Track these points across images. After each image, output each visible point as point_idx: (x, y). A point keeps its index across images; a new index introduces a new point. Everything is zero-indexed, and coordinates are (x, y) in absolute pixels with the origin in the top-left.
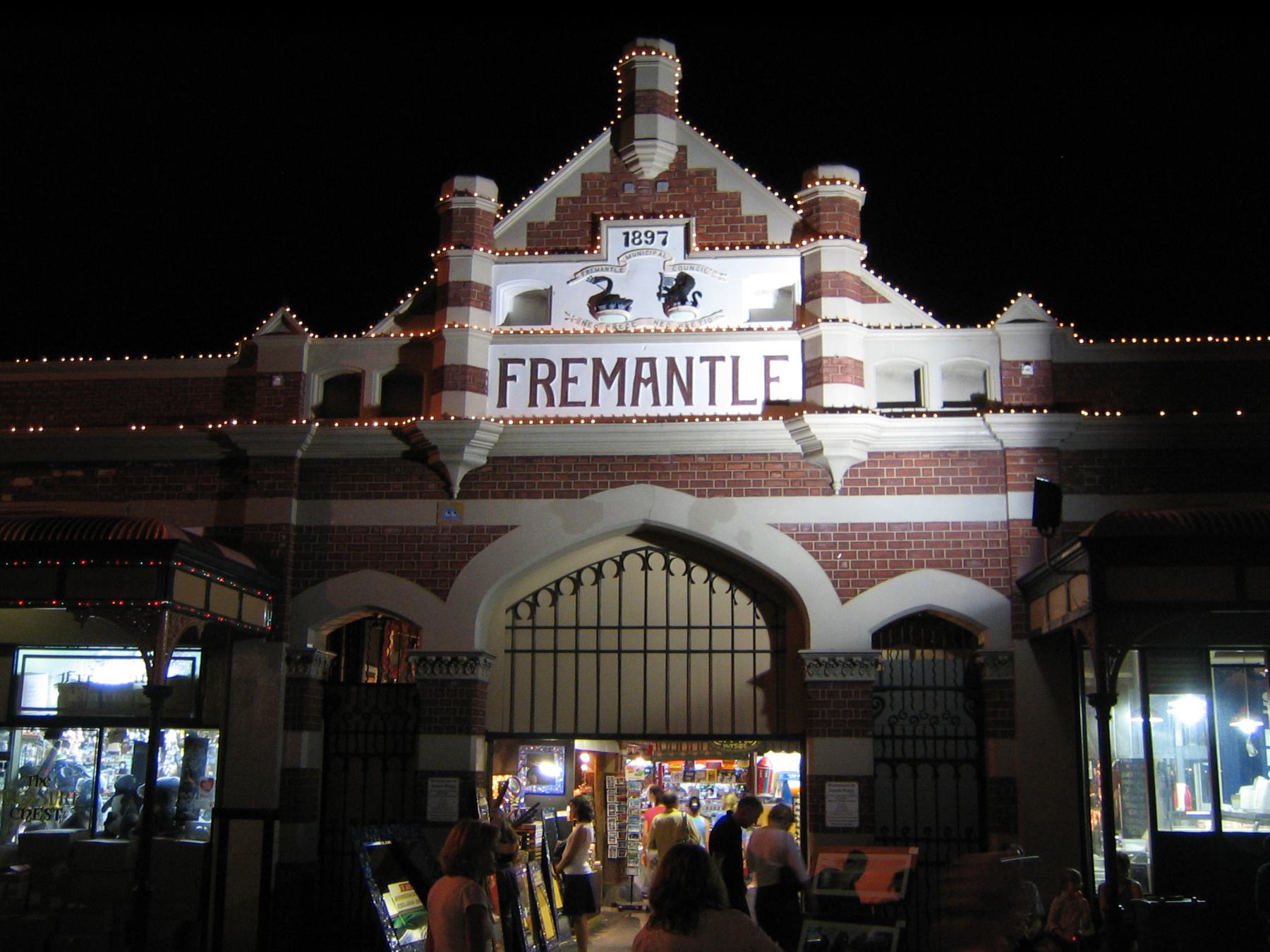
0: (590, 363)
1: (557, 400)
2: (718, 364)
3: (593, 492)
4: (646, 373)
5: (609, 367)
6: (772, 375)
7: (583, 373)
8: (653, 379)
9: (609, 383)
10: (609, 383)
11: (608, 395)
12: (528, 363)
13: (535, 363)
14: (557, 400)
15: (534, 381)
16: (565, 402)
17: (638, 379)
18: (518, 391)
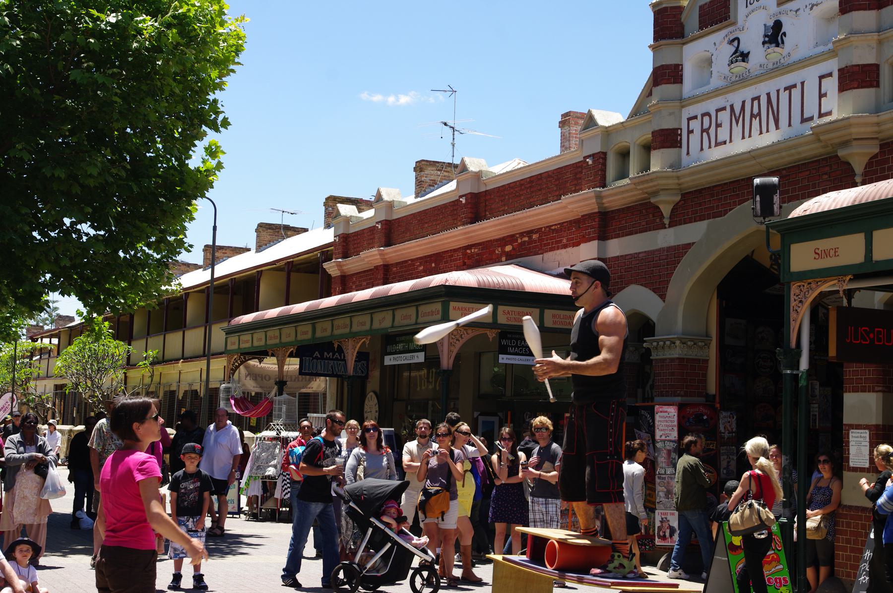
0: (728, 109)
1: (713, 143)
2: (793, 91)
3: (730, 210)
4: (756, 111)
5: (737, 110)
6: (823, 92)
7: (724, 117)
8: (759, 114)
9: (737, 123)
10: (737, 123)
11: (737, 130)
12: (699, 117)
13: (703, 115)
14: (713, 143)
15: (703, 131)
16: (717, 144)
17: (752, 116)
18: (695, 139)
